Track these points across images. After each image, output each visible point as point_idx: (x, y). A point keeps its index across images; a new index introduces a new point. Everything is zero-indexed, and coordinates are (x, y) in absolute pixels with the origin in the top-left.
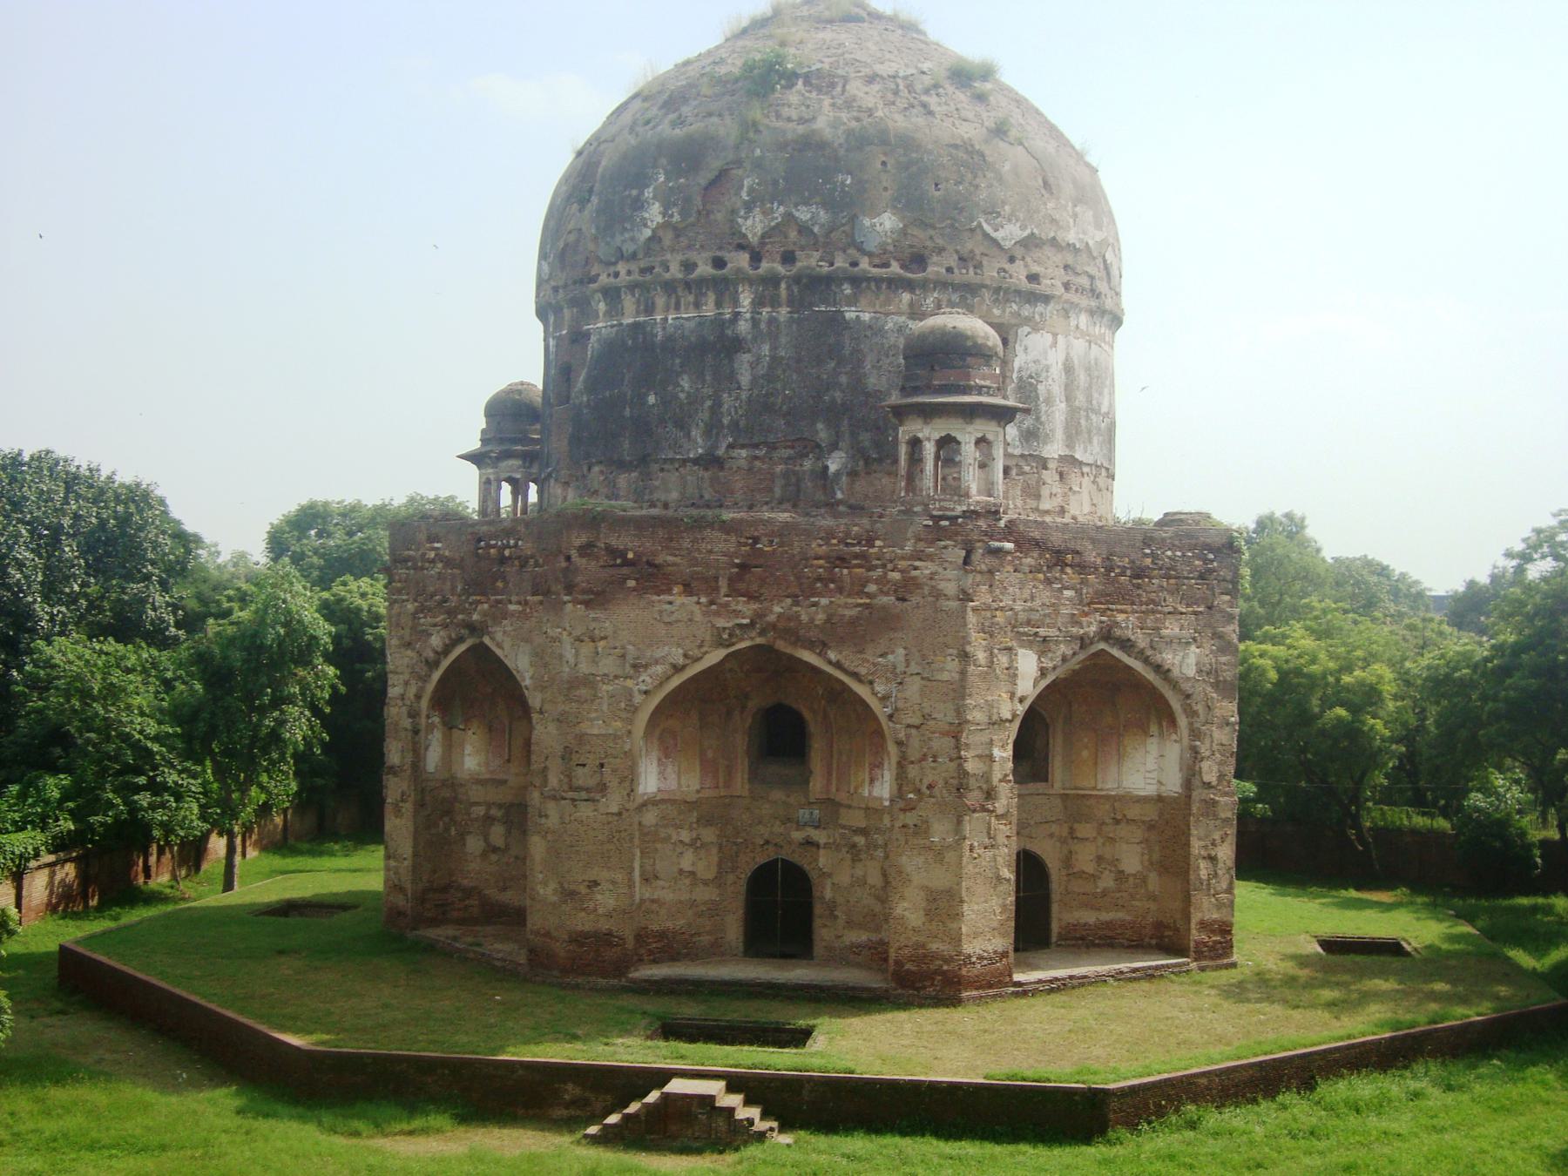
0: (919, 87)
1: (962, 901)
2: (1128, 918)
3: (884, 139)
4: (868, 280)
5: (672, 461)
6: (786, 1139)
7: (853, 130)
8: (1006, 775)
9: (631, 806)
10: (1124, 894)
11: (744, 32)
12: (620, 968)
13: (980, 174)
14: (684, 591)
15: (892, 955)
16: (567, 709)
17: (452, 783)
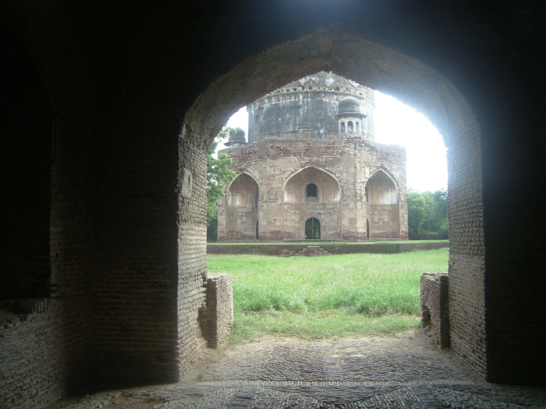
5: (285, 132)
16: (268, 182)
17: (234, 208)
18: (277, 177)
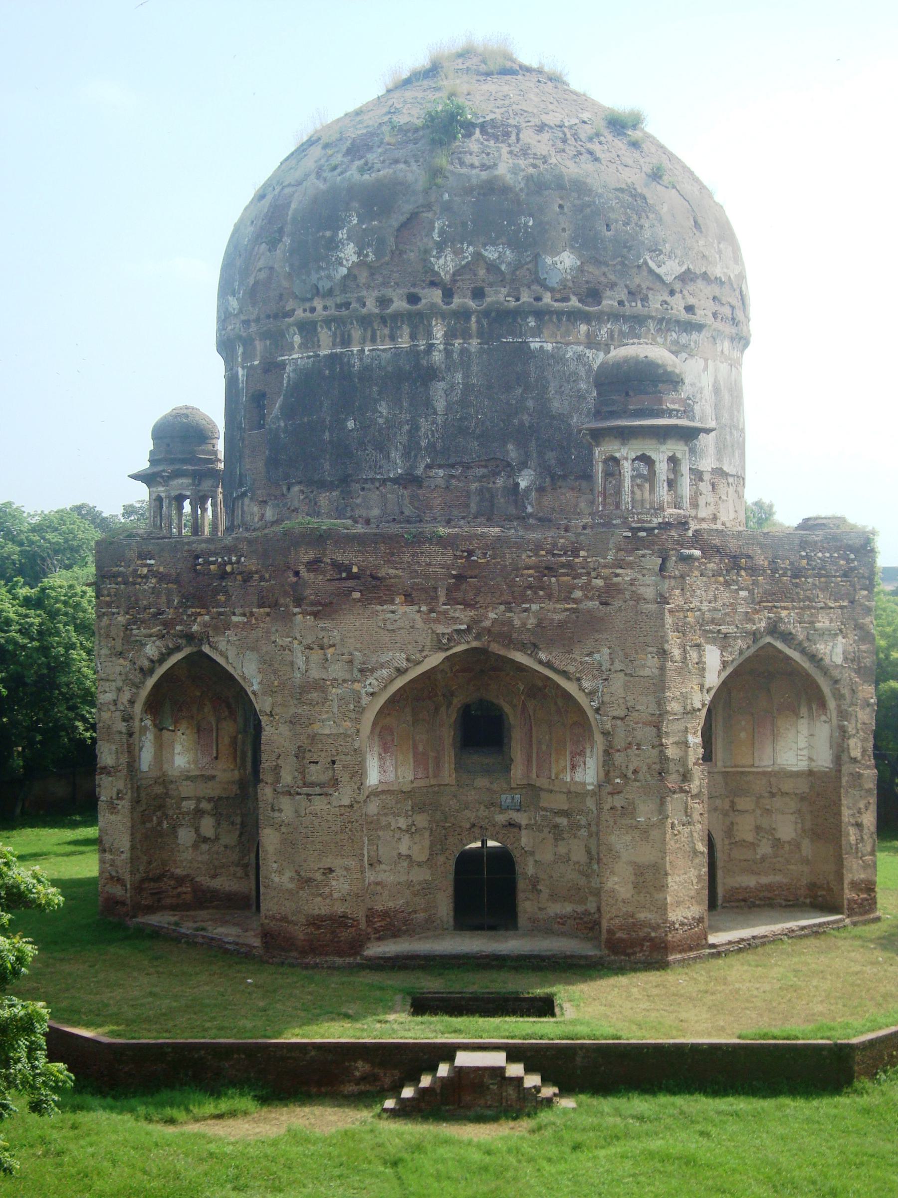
0: (583, 136)
1: (666, 874)
2: (785, 881)
3: (560, 184)
4: (550, 312)
5: (373, 480)
6: (568, 1103)
7: (532, 176)
8: (698, 759)
9: (361, 798)
10: (780, 859)
11: (407, 82)
12: (355, 946)
13: (643, 214)
14: (406, 601)
15: (605, 924)
16: (300, 711)
17: (164, 781)
18: (334, 690)
